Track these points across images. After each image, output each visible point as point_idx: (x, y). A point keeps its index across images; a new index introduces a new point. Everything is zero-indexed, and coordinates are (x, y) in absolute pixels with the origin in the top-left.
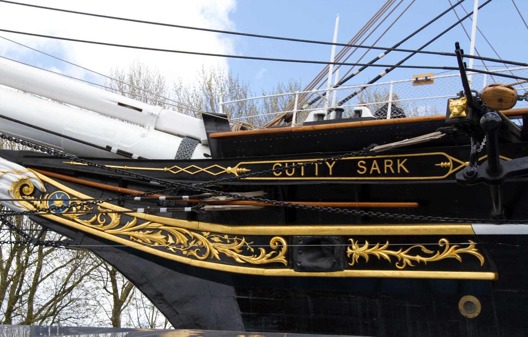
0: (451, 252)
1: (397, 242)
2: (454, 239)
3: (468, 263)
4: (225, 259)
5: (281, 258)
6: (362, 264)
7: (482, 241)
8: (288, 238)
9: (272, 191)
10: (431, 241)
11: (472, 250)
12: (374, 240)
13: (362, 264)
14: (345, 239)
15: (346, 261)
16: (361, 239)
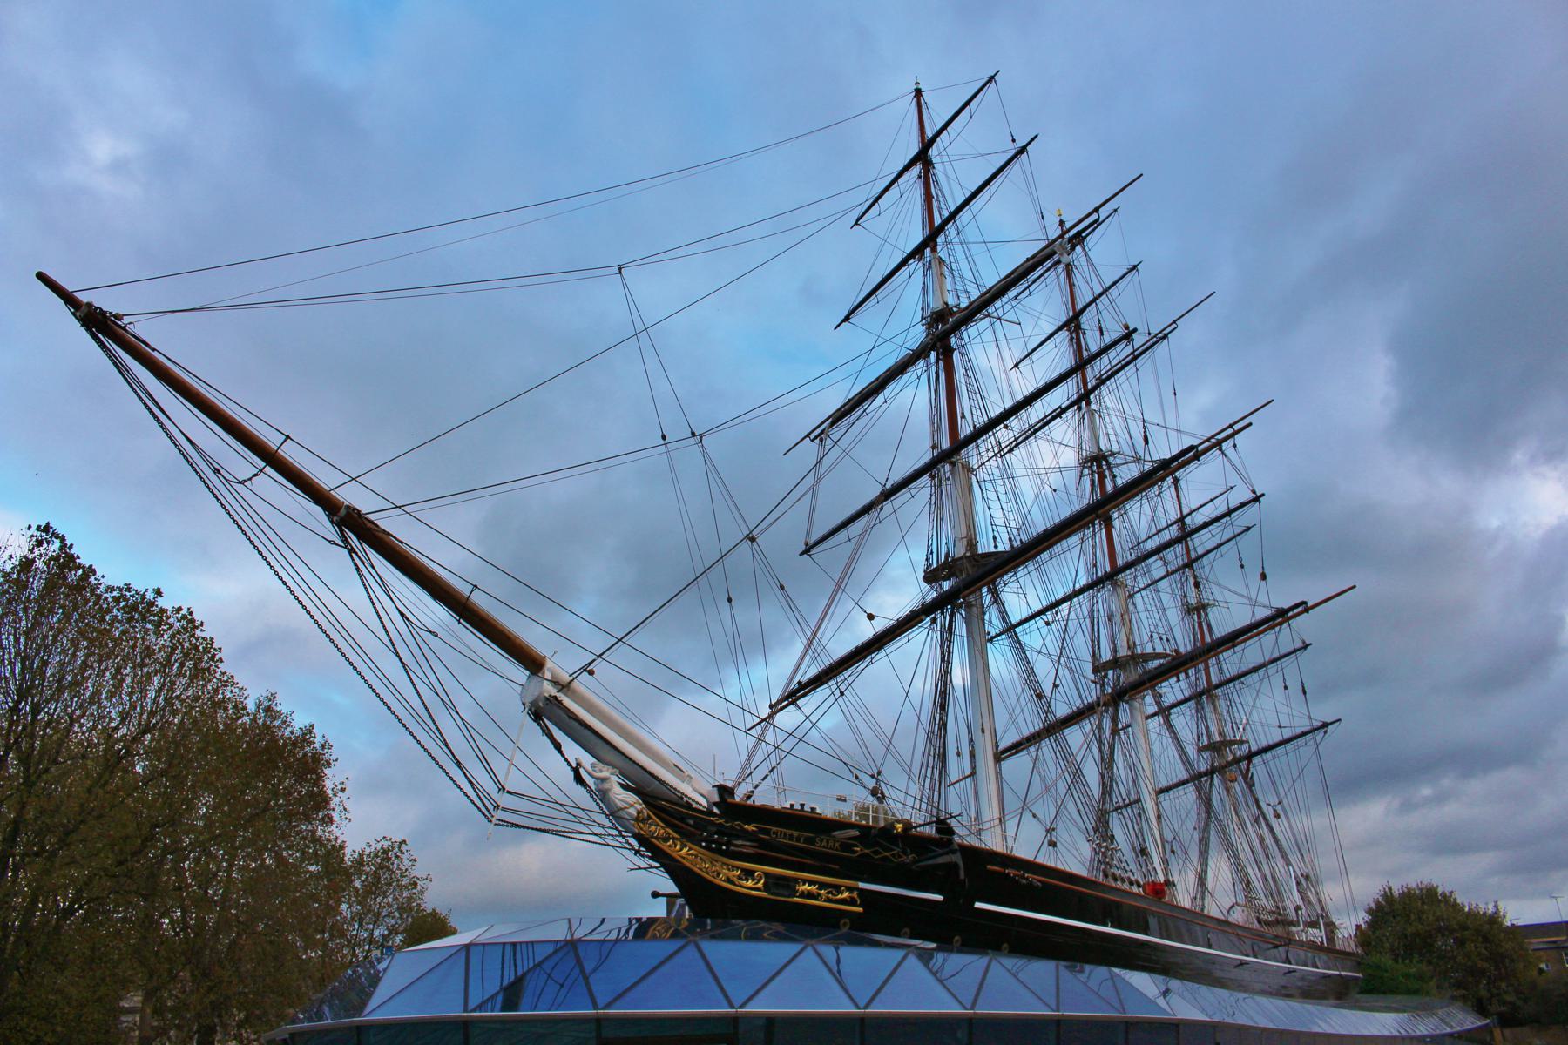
0: (846, 895)
1: (822, 885)
2: (850, 889)
3: (852, 902)
4: (729, 880)
5: (760, 884)
6: (803, 895)
7: (861, 891)
8: (766, 875)
9: (763, 844)
10: (837, 888)
11: (855, 894)
12: (811, 883)
13: (803, 895)
14: (796, 880)
15: (794, 893)
16: (804, 881)
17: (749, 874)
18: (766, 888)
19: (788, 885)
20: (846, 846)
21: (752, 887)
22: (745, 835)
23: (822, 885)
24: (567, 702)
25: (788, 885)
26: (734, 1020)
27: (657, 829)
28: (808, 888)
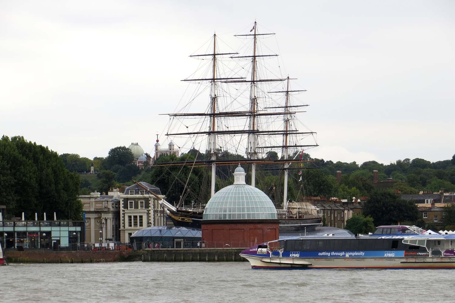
1: (188, 219)
3: (191, 221)
8: (181, 218)
10: (189, 219)
14: (185, 219)
17: (179, 218)
18: (181, 220)
19: (184, 219)
20: (191, 214)
21: (180, 220)
22: (180, 214)
23: (188, 219)
24: (164, 203)
25: (184, 219)
26: (184, 237)
27: (171, 215)
28: (187, 220)
